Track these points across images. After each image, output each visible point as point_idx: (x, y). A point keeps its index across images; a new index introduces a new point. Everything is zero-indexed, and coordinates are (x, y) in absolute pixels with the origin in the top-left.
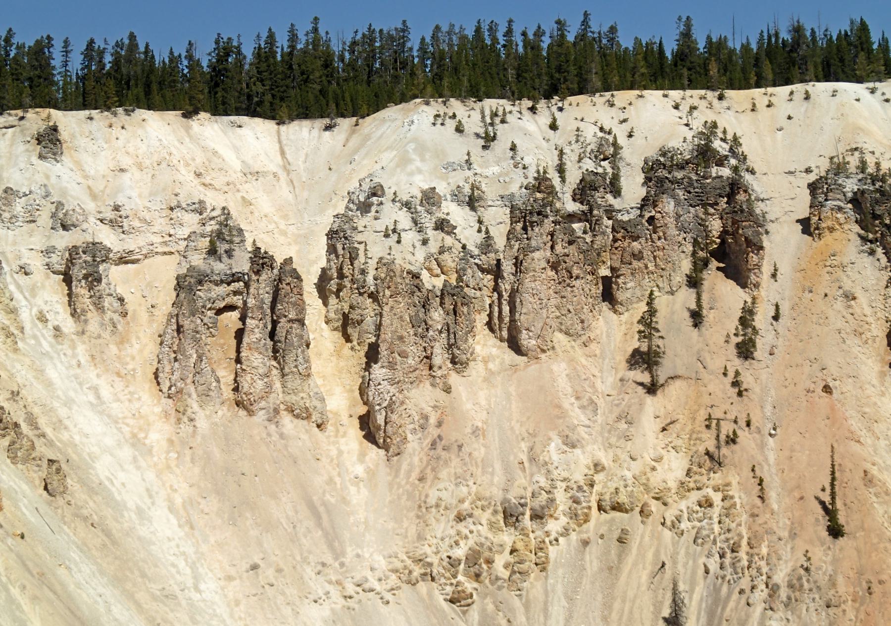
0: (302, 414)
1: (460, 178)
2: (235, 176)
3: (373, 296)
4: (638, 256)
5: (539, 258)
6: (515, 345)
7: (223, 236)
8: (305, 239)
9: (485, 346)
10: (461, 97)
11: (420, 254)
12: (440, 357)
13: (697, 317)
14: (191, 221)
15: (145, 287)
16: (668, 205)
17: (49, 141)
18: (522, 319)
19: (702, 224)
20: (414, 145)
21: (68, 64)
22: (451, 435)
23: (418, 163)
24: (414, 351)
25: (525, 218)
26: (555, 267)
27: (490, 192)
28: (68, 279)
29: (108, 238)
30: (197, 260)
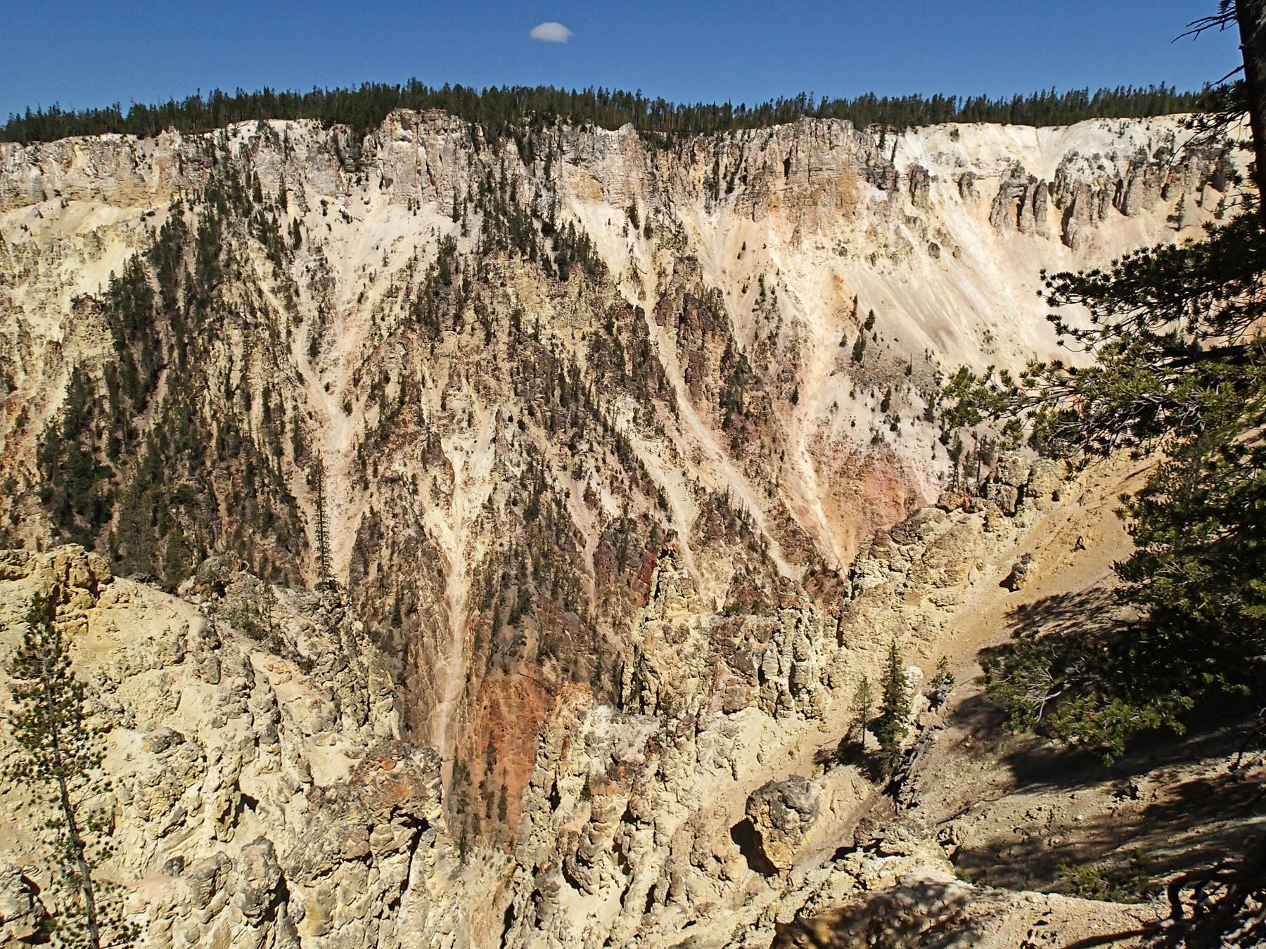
0: (1041, 234)
1: (1109, 150)
2: (1020, 148)
3: (1072, 194)
4: (1179, 179)
5: (1139, 180)
6: (1124, 212)
7: (1016, 171)
8: (1045, 171)
9: (1112, 212)
10: (1111, 118)
11: (1091, 178)
12: (1095, 216)
13: (1199, 203)
14: (1004, 165)
15: (987, 188)
16: (1194, 160)
17: (955, 135)
18: (1129, 202)
19: (1207, 167)
20: (1091, 136)
21: (959, 106)
22: (1097, 243)
23: (1092, 143)
24: (1086, 213)
25: (1135, 165)
26: (1144, 183)
27: (1120, 155)
28: (960, 185)
29: (974, 170)
30: (1006, 178)
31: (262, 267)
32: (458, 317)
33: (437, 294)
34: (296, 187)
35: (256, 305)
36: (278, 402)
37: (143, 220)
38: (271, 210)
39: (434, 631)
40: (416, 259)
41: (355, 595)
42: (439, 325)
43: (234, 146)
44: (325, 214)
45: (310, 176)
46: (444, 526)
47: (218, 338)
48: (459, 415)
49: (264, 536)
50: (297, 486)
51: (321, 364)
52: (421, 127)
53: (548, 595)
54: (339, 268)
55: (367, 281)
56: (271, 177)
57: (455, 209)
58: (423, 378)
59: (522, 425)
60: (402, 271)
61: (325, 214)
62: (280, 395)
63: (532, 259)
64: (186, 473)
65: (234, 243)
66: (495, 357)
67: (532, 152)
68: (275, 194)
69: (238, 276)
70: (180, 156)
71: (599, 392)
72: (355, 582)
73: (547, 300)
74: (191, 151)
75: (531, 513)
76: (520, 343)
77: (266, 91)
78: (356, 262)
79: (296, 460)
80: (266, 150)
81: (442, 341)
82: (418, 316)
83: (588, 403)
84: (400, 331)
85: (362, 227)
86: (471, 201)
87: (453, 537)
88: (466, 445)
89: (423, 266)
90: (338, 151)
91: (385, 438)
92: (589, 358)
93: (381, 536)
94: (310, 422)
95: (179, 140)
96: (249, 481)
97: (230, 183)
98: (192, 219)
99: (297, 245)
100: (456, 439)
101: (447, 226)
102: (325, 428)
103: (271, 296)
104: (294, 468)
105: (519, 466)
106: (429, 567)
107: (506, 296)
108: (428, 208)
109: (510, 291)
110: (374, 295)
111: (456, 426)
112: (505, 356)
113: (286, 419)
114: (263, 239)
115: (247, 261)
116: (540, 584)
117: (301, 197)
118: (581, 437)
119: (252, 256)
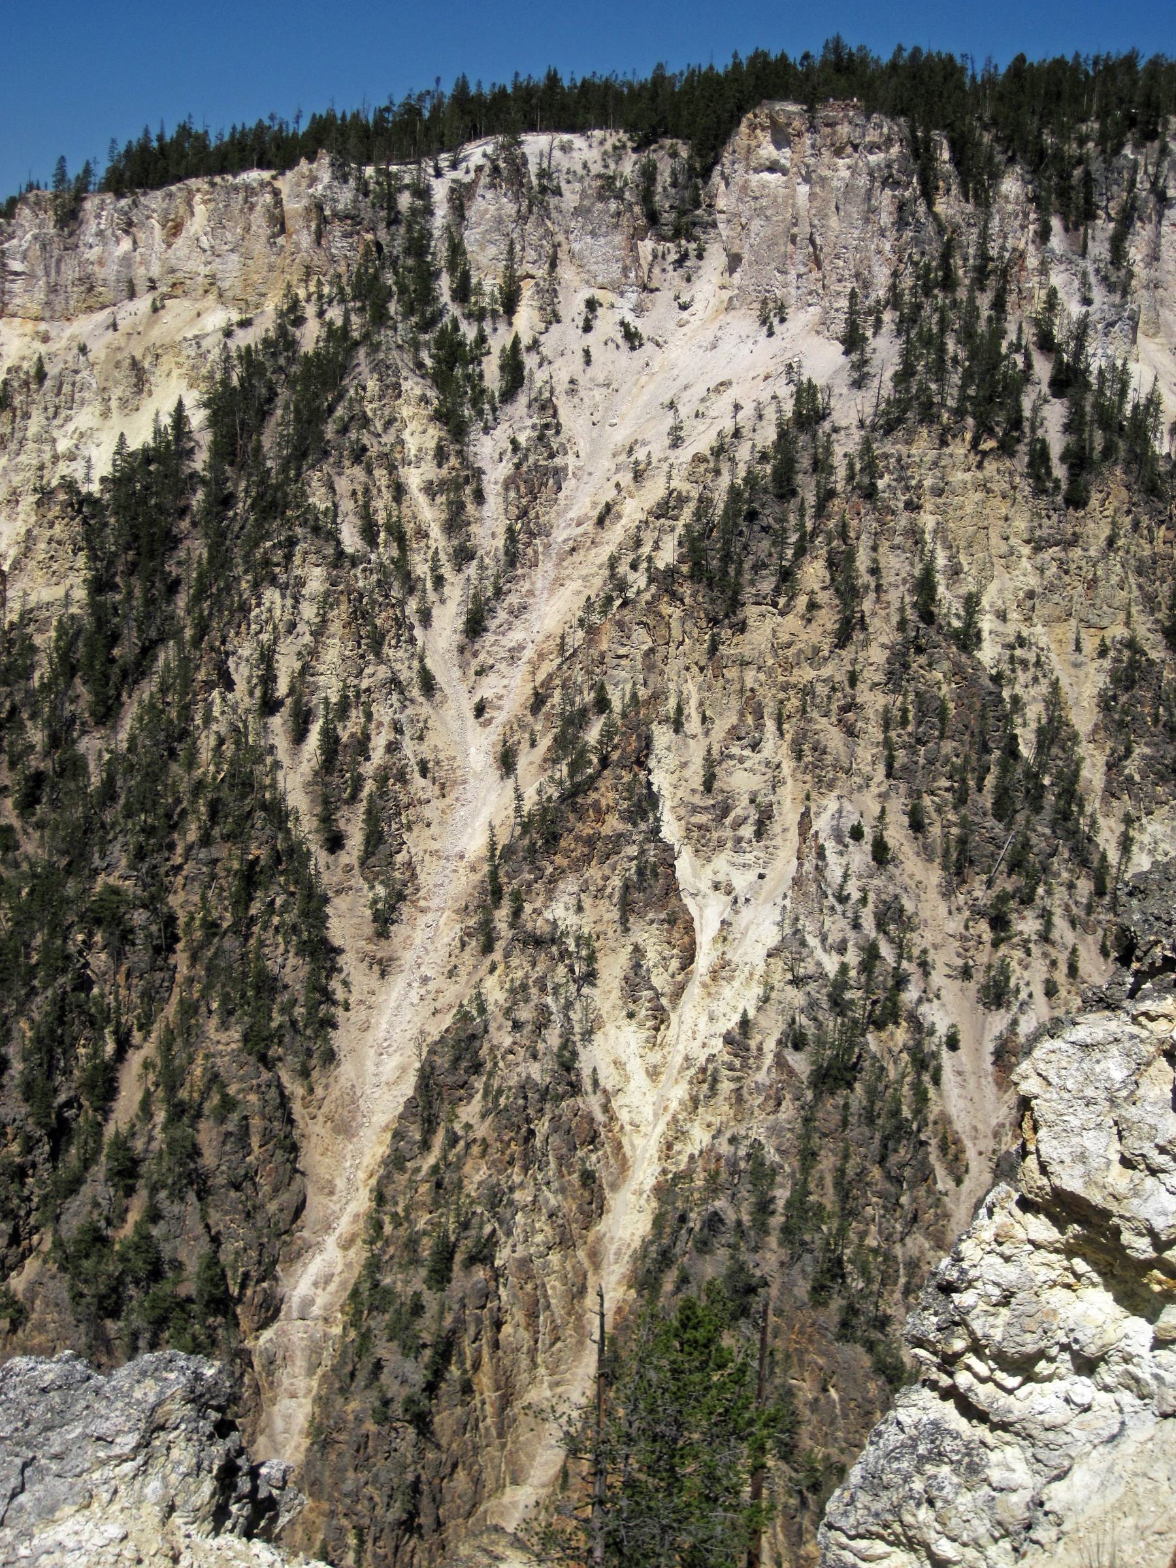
31: (419, 435)
32: (786, 576)
33: (752, 516)
34: (541, 272)
35: (381, 518)
36: (357, 729)
37: (228, 334)
38: (478, 316)
39: (532, 1315)
40: (737, 434)
41: (389, 1192)
42: (737, 589)
43: (440, 190)
44: (587, 328)
45: (576, 247)
46: (636, 1068)
47: (273, 581)
48: (741, 807)
49: (224, 1026)
50: (346, 923)
51: (482, 656)
52: (807, 139)
53: (802, 1289)
54: (583, 446)
55: (626, 478)
56: (492, 251)
57: (852, 325)
58: (679, 710)
59: (881, 853)
60: (698, 459)
61: (587, 328)
62: (369, 716)
63: (1006, 449)
64: (124, 862)
65: (372, 385)
66: (853, 679)
67: (1088, 200)
68: (490, 283)
69: (359, 454)
70: (320, 208)
71: (1110, 793)
72: (396, 1161)
73: (1026, 550)
74: (345, 196)
75: (834, 1075)
76: (920, 650)
77: (553, 79)
78: (620, 436)
79: (362, 864)
80: (489, 195)
81: (742, 627)
82: (696, 564)
83: (1064, 818)
84: (647, 596)
85: (658, 359)
86: (895, 307)
87: (652, 1097)
88: (742, 881)
89: (744, 453)
90: (647, 197)
91: (552, 839)
92: (1106, 703)
93: (477, 1068)
94: (418, 782)
95: (326, 176)
96: (243, 899)
97: (410, 262)
98: (310, 336)
100: (721, 863)
101: (825, 361)
102: (447, 801)
103: (422, 499)
104: (358, 881)
105: (842, 949)
106: (560, 1158)
107: (915, 534)
108: (801, 319)
109: (928, 521)
110: (633, 510)
111: (728, 833)
112: (880, 677)
113: (368, 769)
114: (442, 379)
115: (389, 423)
116: (795, 1258)
117: (549, 295)
118: (1027, 900)
119: (406, 412)
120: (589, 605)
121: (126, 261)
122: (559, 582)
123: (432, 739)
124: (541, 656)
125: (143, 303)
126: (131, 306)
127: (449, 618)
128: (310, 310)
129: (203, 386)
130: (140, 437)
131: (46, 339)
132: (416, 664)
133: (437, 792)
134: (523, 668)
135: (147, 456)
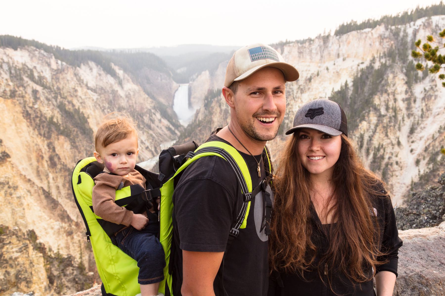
35: (391, 106)
37: (358, 65)
94: (395, 167)
98: (377, 66)
99: (424, 78)
120: (441, 128)
121: (338, 50)
122: (434, 122)
123: (399, 156)
124: (428, 139)
125: (341, 59)
126: (338, 60)
127: (406, 129)
128: (377, 60)
129: (352, 77)
130: (337, 88)
131: (320, 67)
132: (397, 140)
133: (400, 168)
134: (423, 141)
135: (339, 92)
